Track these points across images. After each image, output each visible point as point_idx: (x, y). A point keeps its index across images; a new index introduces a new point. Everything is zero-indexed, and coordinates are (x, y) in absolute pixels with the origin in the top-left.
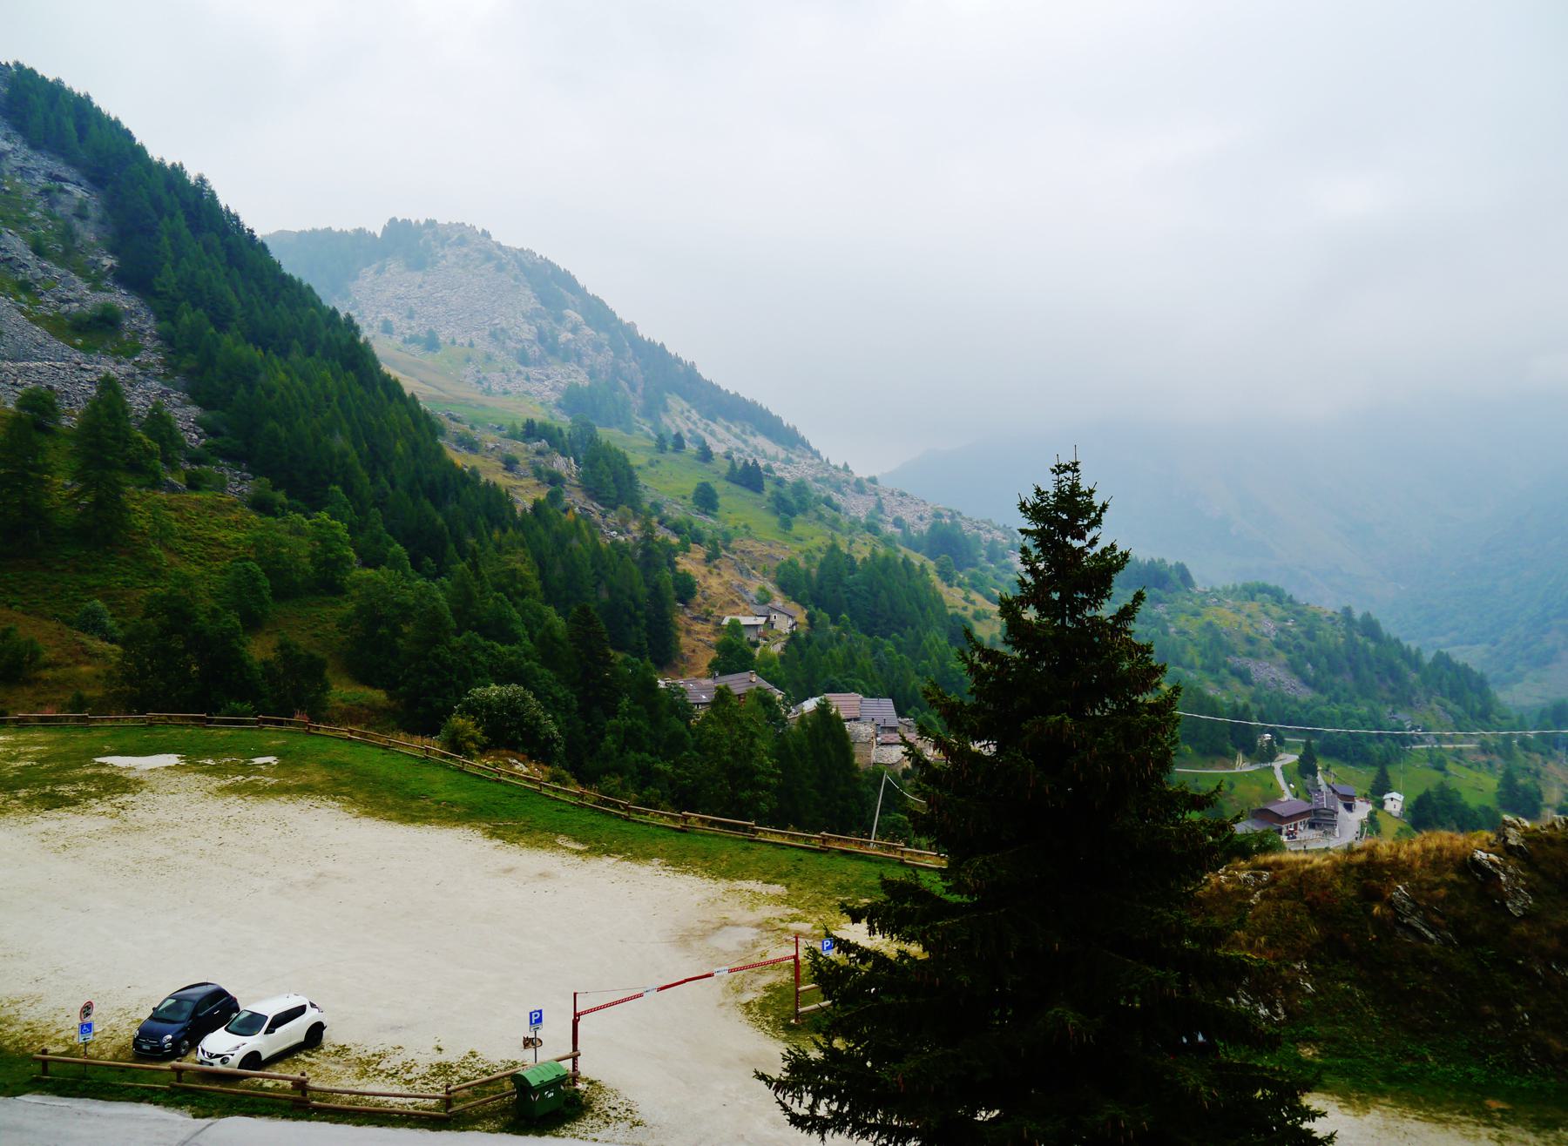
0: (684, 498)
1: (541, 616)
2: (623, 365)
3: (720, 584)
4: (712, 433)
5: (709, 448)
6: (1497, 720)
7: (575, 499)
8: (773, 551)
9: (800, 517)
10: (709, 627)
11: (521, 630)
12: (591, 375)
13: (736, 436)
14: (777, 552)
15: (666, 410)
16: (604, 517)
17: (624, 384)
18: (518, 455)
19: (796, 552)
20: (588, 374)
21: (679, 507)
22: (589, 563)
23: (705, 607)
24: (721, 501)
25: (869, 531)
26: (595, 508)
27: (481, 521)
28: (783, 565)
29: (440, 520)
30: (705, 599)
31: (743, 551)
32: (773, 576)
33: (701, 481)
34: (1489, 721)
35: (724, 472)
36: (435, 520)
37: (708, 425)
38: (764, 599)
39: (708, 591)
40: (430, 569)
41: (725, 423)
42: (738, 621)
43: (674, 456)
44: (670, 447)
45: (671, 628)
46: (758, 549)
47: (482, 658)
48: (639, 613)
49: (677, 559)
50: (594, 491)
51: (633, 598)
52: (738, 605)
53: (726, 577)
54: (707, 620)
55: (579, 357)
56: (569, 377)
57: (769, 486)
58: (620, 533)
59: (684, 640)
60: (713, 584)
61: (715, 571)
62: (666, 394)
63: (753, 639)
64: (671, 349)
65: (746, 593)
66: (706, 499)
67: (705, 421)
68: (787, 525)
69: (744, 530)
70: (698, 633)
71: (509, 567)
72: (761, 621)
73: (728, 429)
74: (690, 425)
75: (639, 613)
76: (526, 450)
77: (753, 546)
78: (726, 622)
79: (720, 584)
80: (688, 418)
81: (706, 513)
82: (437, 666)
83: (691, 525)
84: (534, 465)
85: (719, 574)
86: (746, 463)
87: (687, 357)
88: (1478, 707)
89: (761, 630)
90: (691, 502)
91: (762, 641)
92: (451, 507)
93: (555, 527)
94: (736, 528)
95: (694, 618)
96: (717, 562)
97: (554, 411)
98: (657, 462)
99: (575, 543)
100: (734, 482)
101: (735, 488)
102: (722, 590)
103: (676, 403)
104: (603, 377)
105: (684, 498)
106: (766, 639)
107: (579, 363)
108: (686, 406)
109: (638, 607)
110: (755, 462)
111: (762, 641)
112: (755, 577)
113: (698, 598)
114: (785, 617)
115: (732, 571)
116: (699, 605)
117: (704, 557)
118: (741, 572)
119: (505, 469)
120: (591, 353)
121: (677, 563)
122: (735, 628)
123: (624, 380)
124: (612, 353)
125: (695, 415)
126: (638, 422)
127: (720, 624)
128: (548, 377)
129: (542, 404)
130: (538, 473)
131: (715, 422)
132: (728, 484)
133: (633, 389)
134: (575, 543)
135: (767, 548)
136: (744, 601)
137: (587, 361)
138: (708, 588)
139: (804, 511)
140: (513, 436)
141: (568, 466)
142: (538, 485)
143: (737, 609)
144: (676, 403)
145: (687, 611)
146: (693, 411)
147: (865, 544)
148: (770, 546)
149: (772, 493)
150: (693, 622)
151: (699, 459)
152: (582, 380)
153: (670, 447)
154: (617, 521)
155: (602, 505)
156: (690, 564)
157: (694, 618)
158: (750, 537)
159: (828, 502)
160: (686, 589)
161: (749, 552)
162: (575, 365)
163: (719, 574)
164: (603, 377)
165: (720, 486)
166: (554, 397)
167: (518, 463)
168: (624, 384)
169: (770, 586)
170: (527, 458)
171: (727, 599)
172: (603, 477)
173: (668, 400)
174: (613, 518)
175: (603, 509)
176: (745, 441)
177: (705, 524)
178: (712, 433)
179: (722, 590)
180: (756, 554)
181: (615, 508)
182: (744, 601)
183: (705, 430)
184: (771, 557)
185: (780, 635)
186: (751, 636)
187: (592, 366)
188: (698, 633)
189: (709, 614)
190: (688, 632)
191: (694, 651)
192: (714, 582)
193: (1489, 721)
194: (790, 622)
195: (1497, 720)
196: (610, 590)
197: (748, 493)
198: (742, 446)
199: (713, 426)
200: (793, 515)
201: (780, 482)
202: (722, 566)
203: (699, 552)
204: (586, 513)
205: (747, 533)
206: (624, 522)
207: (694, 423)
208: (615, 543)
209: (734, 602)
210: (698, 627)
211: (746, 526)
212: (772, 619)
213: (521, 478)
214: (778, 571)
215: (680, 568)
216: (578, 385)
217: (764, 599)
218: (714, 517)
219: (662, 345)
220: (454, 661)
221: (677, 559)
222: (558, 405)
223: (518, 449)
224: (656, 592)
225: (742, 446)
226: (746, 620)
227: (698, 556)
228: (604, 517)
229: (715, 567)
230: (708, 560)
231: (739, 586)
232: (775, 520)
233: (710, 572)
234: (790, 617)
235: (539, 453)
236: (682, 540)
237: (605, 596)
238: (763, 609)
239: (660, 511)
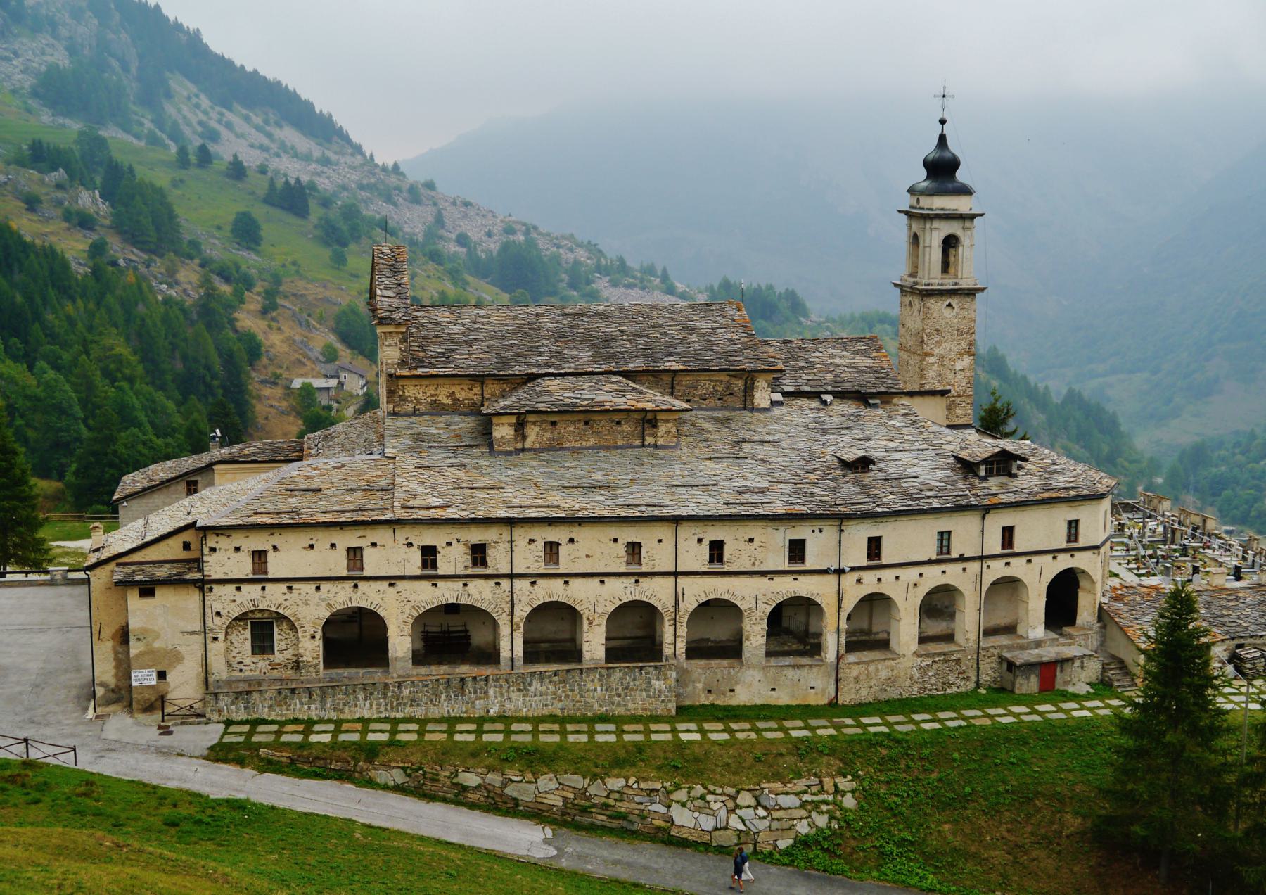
0: (219, 228)
1: (154, 402)
2: (111, 36)
3: (283, 341)
4: (229, 126)
5: (241, 163)
6: (1126, 464)
7: (118, 249)
8: (328, 294)
9: (352, 247)
10: (278, 391)
11: (142, 417)
12: (72, 50)
13: (257, 128)
14: (331, 294)
15: (169, 95)
16: (148, 266)
17: (115, 63)
18: (36, 189)
19: (355, 293)
20: (67, 49)
21: (217, 242)
22: (163, 333)
23: (271, 369)
24: (267, 231)
25: (433, 261)
26: (136, 255)
27: (52, 292)
28: (344, 312)
29: (19, 299)
30: (270, 359)
31: (295, 295)
32: (332, 323)
33: (246, 210)
34: (1115, 465)
35: (262, 192)
36: (14, 297)
37: (222, 114)
38: (330, 356)
39: (273, 351)
40: (18, 349)
41: (244, 112)
42: (310, 385)
43: (198, 171)
44: (193, 158)
45: (247, 397)
46: (313, 292)
47: (145, 451)
48: (216, 383)
49: (236, 315)
50: (133, 237)
51: (208, 368)
52: (304, 365)
53: (288, 332)
54: (275, 384)
55: (53, 25)
56: (43, 53)
57: (316, 212)
58: (170, 286)
59: (260, 409)
60: (275, 341)
61: (273, 324)
62: (168, 74)
63: (325, 402)
64: (170, 12)
65: (311, 349)
66: (247, 232)
67: (218, 109)
68: (340, 260)
69: (293, 268)
70: (268, 399)
71: (113, 352)
72: (333, 383)
73: (247, 119)
74: (202, 117)
75: (216, 383)
76: (42, 181)
77: (306, 289)
78: (297, 383)
79: (283, 341)
80: (197, 106)
81: (249, 248)
82: (116, 460)
83: (238, 268)
84: (59, 203)
85: (279, 329)
86: (287, 182)
87: (189, 23)
88: (1105, 449)
89: (332, 393)
90: (228, 234)
91: (335, 405)
92: (17, 277)
93: (119, 292)
94: (284, 266)
95: (262, 382)
96: (274, 314)
97: (30, 102)
98: (182, 181)
99: (141, 309)
100: (273, 205)
101: (277, 213)
102: (287, 349)
103: (181, 86)
104: (86, 52)
105: (219, 228)
106: (338, 402)
107: (55, 36)
108: (194, 89)
109: (214, 376)
110: (298, 180)
111: (335, 405)
112: (316, 328)
113: (264, 360)
114: (356, 377)
115: (291, 323)
116: (265, 367)
117: (259, 307)
118: (300, 324)
119: (27, 210)
120: (68, 20)
121: (236, 320)
122: (307, 391)
123: (118, 60)
124: (96, 22)
125: (205, 102)
126: (136, 114)
127: (289, 388)
128: (16, 54)
129: (14, 92)
130: (67, 216)
131: (230, 110)
132: (266, 208)
133: (126, 69)
134: (141, 309)
135: (322, 290)
136: (309, 359)
137: (64, 32)
138: (272, 346)
139: (356, 238)
140: (20, 162)
141: (94, 202)
142: (69, 229)
143: (303, 371)
144: (181, 86)
145: (254, 374)
146: (203, 96)
147: (429, 277)
148: (325, 287)
149: (321, 219)
150: (261, 386)
151: (228, 176)
152: (61, 58)
153: (193, 158)
154: (163, 270)
155: (142, 250)
156: (247, 320)
157: (262, 382)
158: (302, 277)
159: (384, 225)
160: (254, 350)
161: (302, 295)
162: (49, 37)
163: (279, 329)
164: (86, 52)
165: (260, 212)
166: (28, 82)
167: (40, 202)
168: (115, 63)
169: (332, 339)
170: (47, 194)
171: (293, 359)
172: (141, 218)
173: (171, 83)
174: (159, 266)
175: (145, 257)
176: (269, 136)
177: (249, 261)
178: (229, 126)
179: (287, 349)
180: (310, 298)
181: (161, 256)
182: (309, 359)
183: (219, 122)
184: (326, 300)
185: (352, 396)
186: (324, 400)
187: (70, 38)
188: (268, 399)
189: (278, 377)
190: (259, 398)
191: (267, 418)
192: (276, 339)
193: (1115, 465)
194: (362, 382)
195: (1126, 464)
196: (185, 358)
197: (293, 219)
198: (266, 142)
199: (229, 116)
200: (345, 245)
201: (326, 203)
202: (280, 318)
203: (254, 301)
204: (133, 264)
205: (297, 272)
206: (171, 273)
207: (205, 113)
208: (168, 301)
209: (300, 361)
210: (267, 392)
211: (294, 263)
212: (342, 379)
213: (48, 220)
214: (338, 319)
215: (238, 325)
216: (58, 66)
217: (330, 356)
218: (258, 253)
219: (157, 7)
220: (128, 455)
221: (236, 315)
222: (35, 94)
223: (30, 179)
224: (229, 359)
225: (266, 142)
226: (319, 383)
227: (252, 307)
228: (148, 266)
229: (273, 319)
230: (264, 312)
231: (302, 342)
232: (326, 253)
233: (270, 327)
234: (362, 376)
235: (59, 186)
236: (236, 290)
237: (179, 366)
238: (330, 368)
239: (199, 251)
